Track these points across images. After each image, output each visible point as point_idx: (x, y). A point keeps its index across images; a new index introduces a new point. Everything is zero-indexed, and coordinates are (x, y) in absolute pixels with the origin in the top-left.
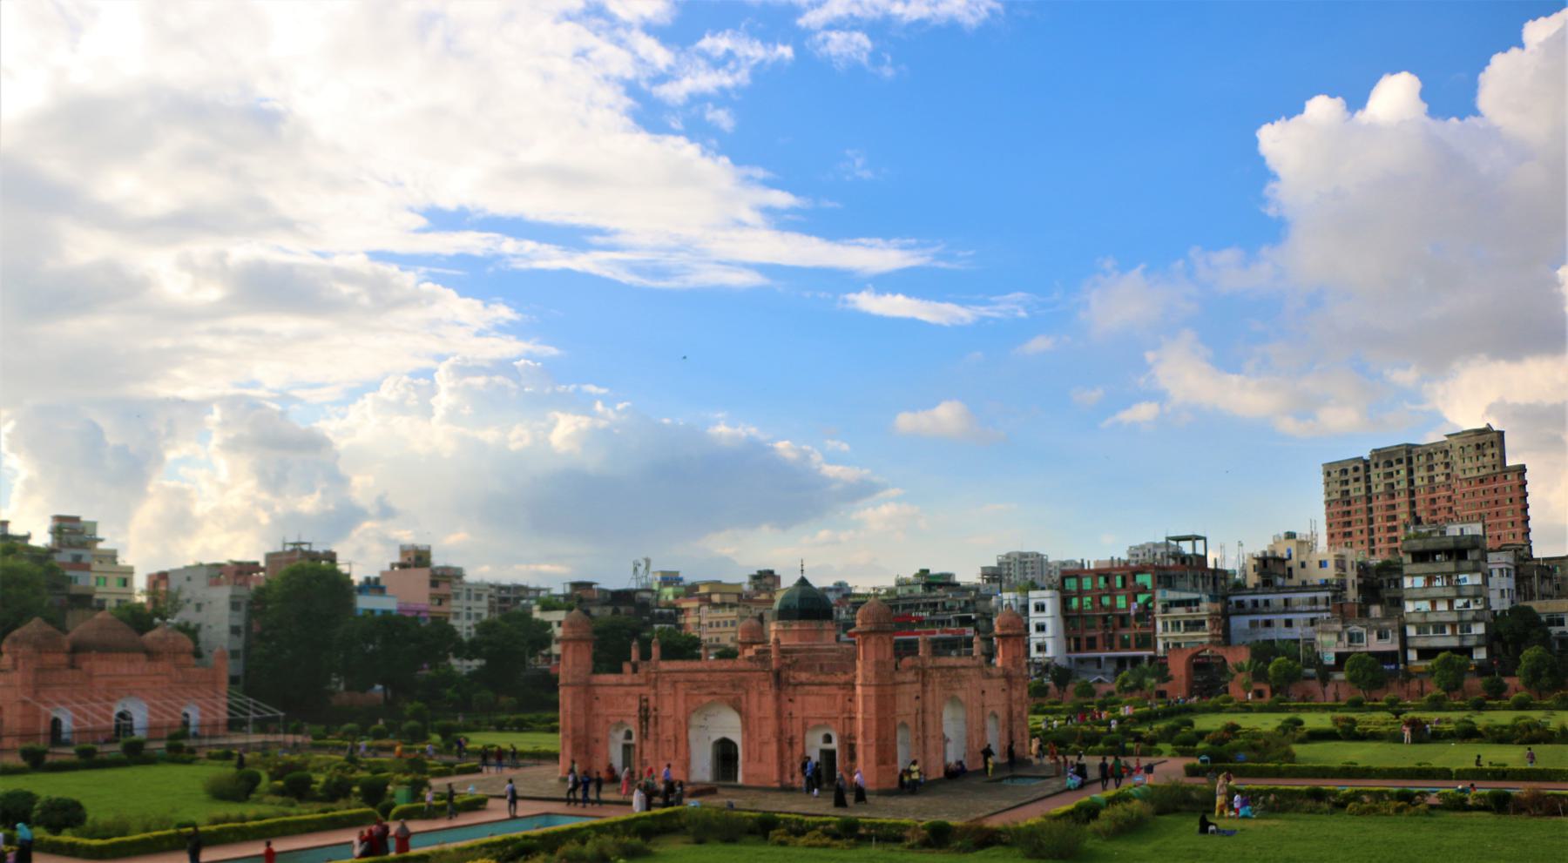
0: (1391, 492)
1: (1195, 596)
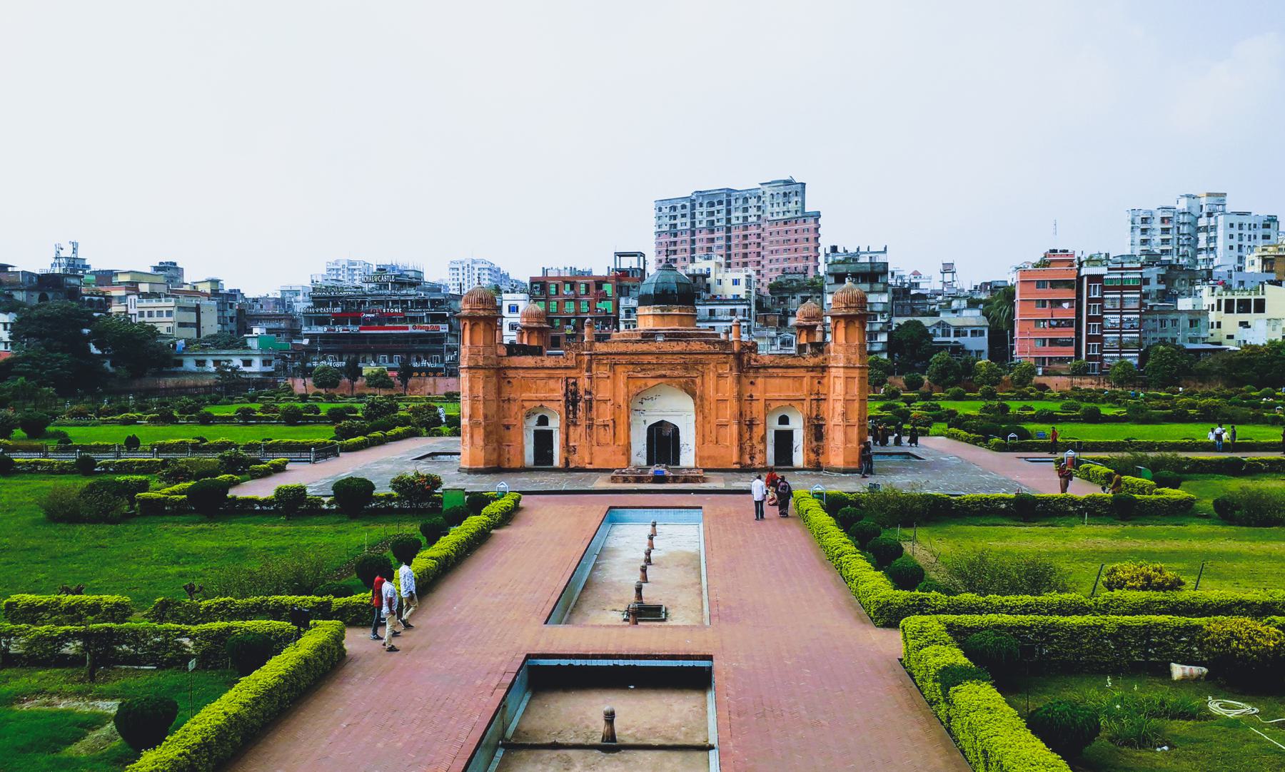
0: (711, 227)
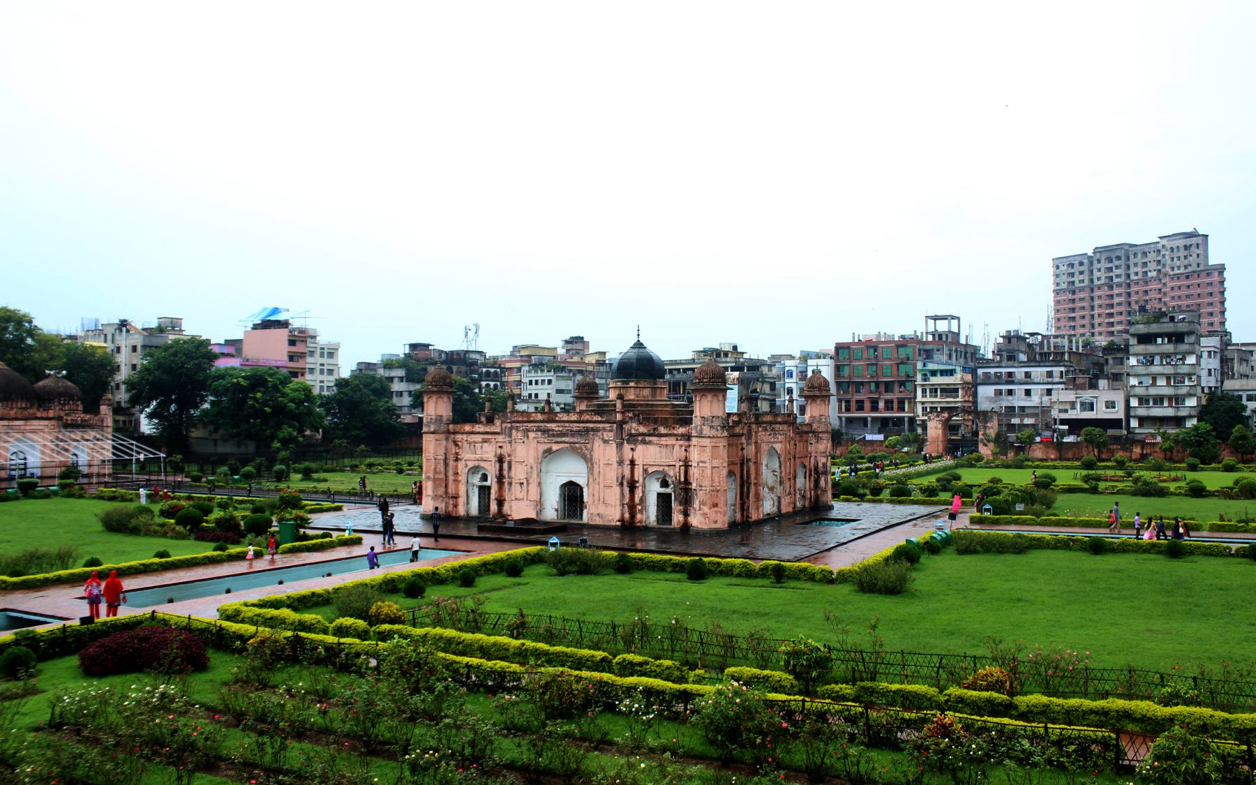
1: (950, 367)
